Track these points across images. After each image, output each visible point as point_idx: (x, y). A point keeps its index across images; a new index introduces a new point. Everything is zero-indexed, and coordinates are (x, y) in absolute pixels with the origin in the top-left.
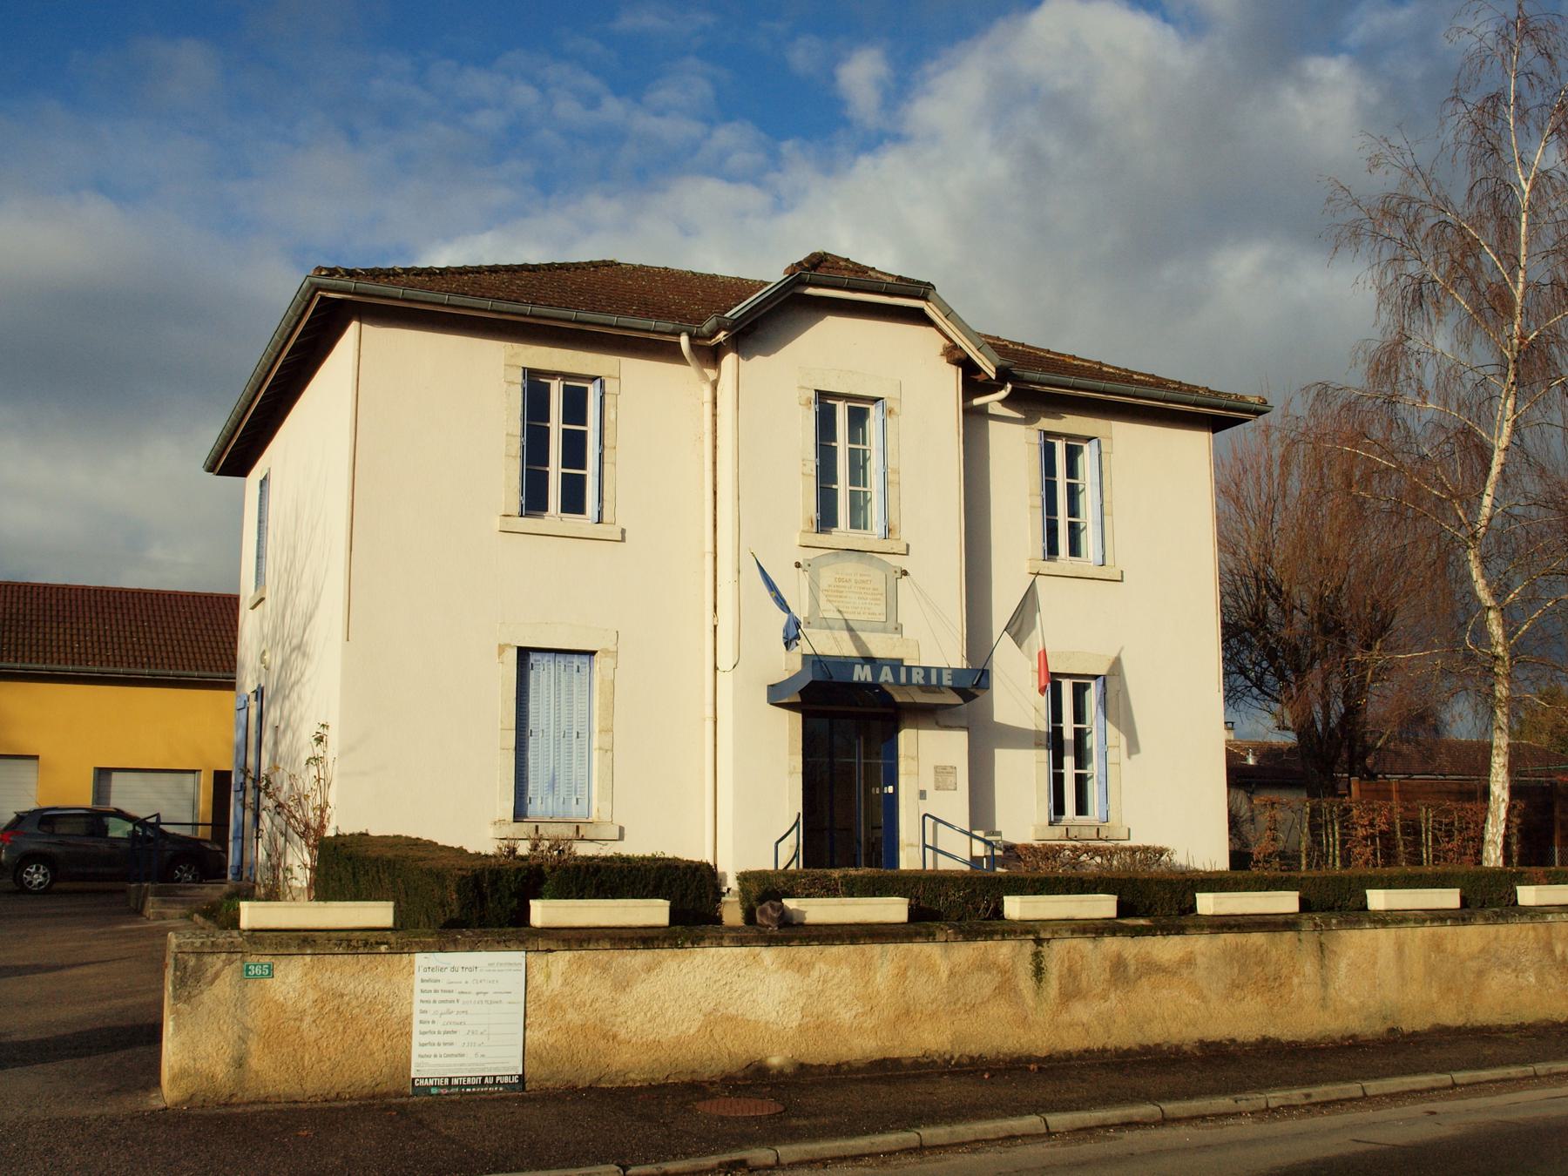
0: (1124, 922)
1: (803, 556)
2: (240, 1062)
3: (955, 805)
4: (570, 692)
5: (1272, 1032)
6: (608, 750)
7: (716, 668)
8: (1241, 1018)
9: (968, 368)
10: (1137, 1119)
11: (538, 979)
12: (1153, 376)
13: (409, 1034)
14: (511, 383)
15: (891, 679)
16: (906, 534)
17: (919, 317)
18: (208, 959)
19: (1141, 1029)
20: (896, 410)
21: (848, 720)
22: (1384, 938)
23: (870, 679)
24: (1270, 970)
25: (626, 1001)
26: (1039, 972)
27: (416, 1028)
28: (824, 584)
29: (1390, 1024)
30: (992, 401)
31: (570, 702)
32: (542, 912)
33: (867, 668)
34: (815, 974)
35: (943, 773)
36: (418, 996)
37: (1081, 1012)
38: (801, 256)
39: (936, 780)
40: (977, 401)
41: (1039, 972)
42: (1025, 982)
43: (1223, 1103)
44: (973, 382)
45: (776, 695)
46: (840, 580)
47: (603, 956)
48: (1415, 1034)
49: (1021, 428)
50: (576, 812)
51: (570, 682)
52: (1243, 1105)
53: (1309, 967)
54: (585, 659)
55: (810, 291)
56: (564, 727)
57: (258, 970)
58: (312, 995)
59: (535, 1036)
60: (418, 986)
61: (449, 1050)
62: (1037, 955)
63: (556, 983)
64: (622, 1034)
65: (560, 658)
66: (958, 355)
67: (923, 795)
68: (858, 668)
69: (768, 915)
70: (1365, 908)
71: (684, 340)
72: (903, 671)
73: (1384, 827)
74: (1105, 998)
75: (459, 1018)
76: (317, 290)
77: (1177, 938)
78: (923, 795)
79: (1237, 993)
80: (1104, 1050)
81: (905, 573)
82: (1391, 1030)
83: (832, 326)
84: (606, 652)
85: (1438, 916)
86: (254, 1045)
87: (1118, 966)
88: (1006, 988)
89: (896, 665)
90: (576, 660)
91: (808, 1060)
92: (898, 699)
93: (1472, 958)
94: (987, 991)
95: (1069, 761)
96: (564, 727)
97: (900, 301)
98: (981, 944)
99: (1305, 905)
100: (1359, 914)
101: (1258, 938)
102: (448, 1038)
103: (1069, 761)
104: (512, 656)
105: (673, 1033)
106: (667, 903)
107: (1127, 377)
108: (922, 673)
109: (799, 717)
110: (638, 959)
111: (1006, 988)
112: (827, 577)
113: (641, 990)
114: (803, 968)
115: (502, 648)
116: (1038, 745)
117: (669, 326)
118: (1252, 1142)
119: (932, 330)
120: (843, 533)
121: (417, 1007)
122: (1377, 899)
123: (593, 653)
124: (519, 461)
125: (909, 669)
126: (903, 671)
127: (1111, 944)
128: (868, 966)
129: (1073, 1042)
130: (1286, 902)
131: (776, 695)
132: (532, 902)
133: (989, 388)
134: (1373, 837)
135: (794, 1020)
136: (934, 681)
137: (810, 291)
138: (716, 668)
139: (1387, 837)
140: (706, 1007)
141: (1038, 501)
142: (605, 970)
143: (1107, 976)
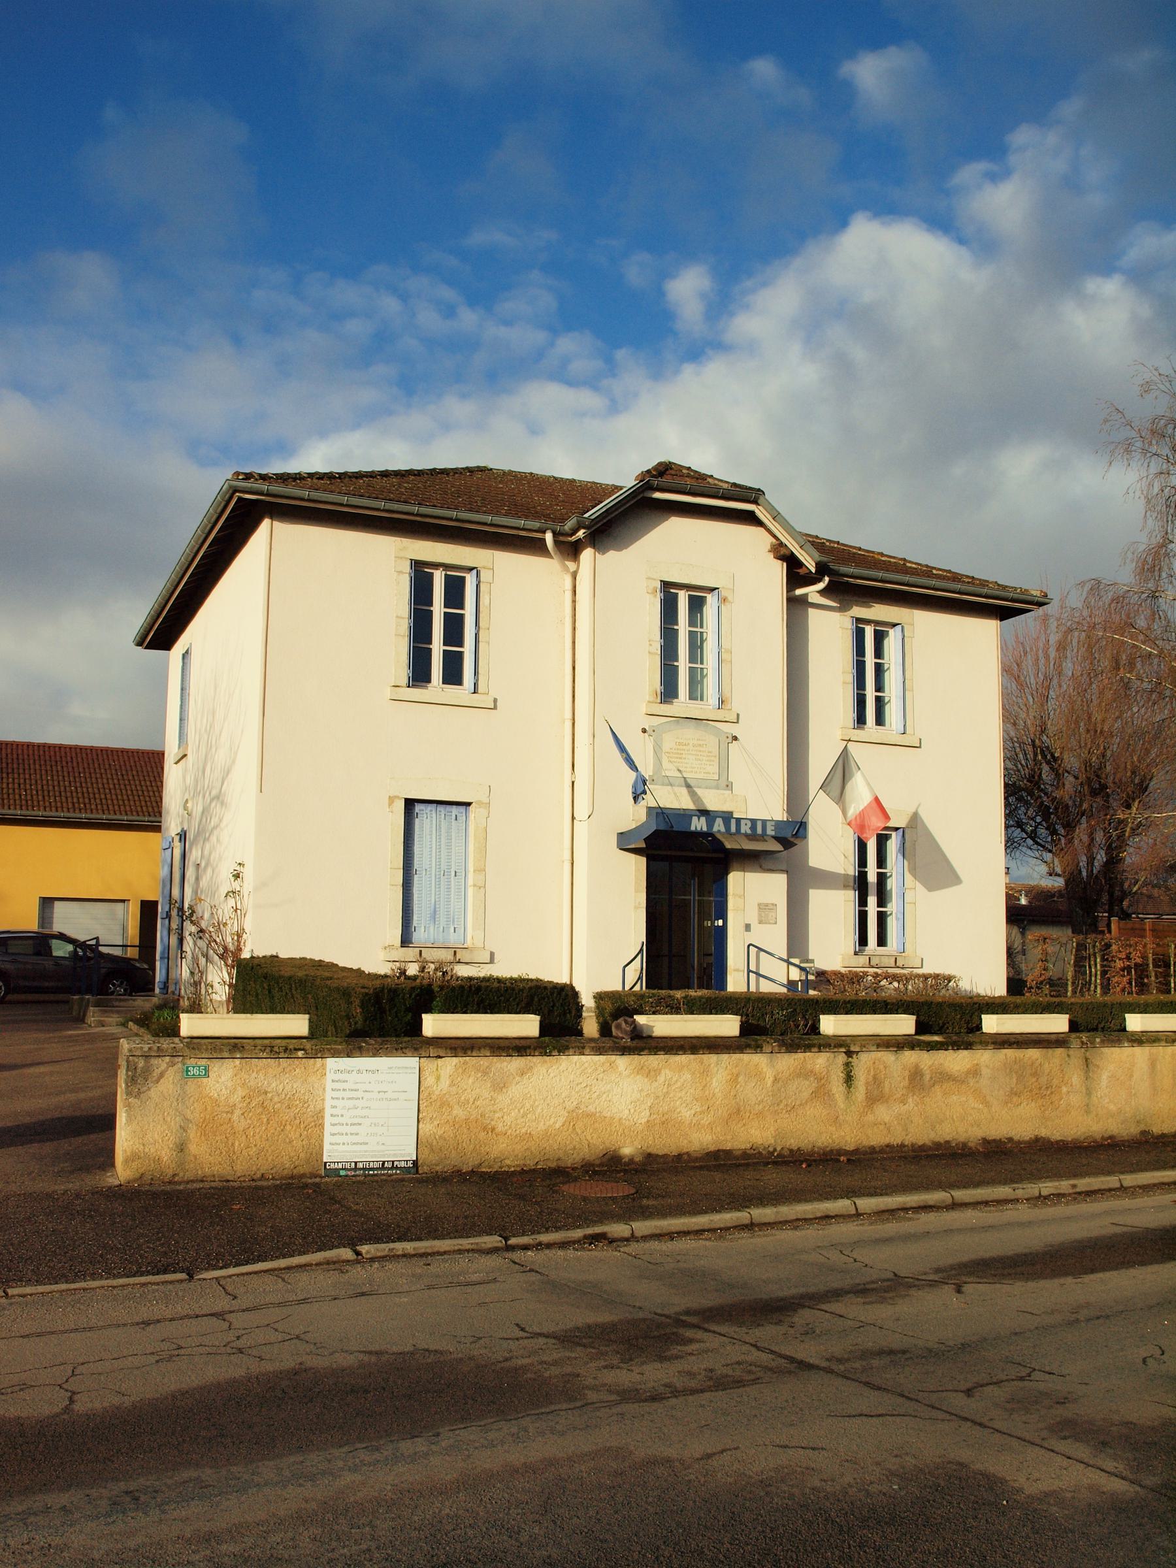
0: (922, 1038)
1: (649, 723)
2: (181, 1148)
3: (775, 937)
4: (449, 838)
5: (1044, 1133)
6: (481, 887)
7: (573, 818)
8: (1019, 1121)
9: (792, 562)
10: (931, 1203)
11: (429, 1080)
12: (949, 571)
13: (322, 1126)
14: (400, 572)
15: (723, 829)
16: (737, 705)
17: (750, 519)
18: (154, 1061)
19: (933, 1128)
20: (730, 598)
21: (686, 864)
22: (1140, 1054)
23: (705, 829)
24: (1043, 1080)
25: (503, 1099)
26: (849, 1079)
27: (328, 1120)
29: (1142, 1127)
30: (812, 592)
31: (449, 846)
32: (433, 1024)
33: (703, 819)
34: (661, 1079)
35: (765, 910)
36: (329, 1094)
37: (883, 1113)
38: (650, 465)
39: (760, 915)
40: (799, 592)
41: (849, 1079)
43: (1003, 1191)
44: (796, 575)
45: (625, 842)
46: (680, 744)
47: (484, 1062)
48: (1163, 1135)
49: (836, 616)
50: (453, 939)
51: (449, 828)
52: (1020, 1193)
53: (1076, 1079)
54: (462, 809)
55: (658, 495)
57: (196, 1071)
58: (240, 1092)
59: (427, 1128)
60: (329, 1085)
61: (355, 1139)
62: (847, 1064)
63: (445, 1084)
64: (500, 1128)
65: (441, 808)
66: (783, 551)
67: (748, 927)
68: (695, 819)
70: (1124, 1030)
71: (549, 537)
72: (733, 822)
73: (1139, 961)
74: (904, 1102)
75: (365, 1112)
76: (235, 491)
77: (965, 1052)
78: (748, 927)
79: (1015, 1099)
80: (902, 1145)
81: (735, 738)
82: (1143, 1133)
83: (676, 525)
84: (480, 803)
86: (193, 1133)
87: (915, 1077)
88: (821, 1092)
89: (727, 817)
90: (455, 810)
91: (654, 1150)
92: (728, 846)
94: (806, 1095)
95: (872, 901)
97: (735, 505)
98: (800, 1056)
99: (1074, 1026)
100: (1118, 1034)
101: (1033, 1054)
102: (355, 1129)
103: (872, 901)
104: (402, 804)
105: (541, 1127)
106: (538, 1018)
107: (928, 572)
109: (643, 860)
110: (514, 1064)
111: (821, 1092)
112: (668, 742)
113: (515, 1091)
114: (652, 1074)
115: (392, 800)
116: (845, 887)
117: (536, 525)
119: (761, 529)
120: (682, 704)
121: (328, 1103)
122: (1135, 1022)
123: (469, 804)
124: (407, 639)
125: (738, 820)
126: (733, 822)
127: (910, 1057)
128: (706, 1072)
129: (876, 1138)
130: (1058, 1023)
131: (625, 842)
132: (424, 1016)
133: (810, 580)
134: (1129, 968)
135: (643, 1117)
136: (759, 831)
137: (658, 495)
138: (573, 818)
139: (1141, 969)
140: (570, 1105)
141: (850, 677)
142: (485, 1073)
143: (906, 1083)
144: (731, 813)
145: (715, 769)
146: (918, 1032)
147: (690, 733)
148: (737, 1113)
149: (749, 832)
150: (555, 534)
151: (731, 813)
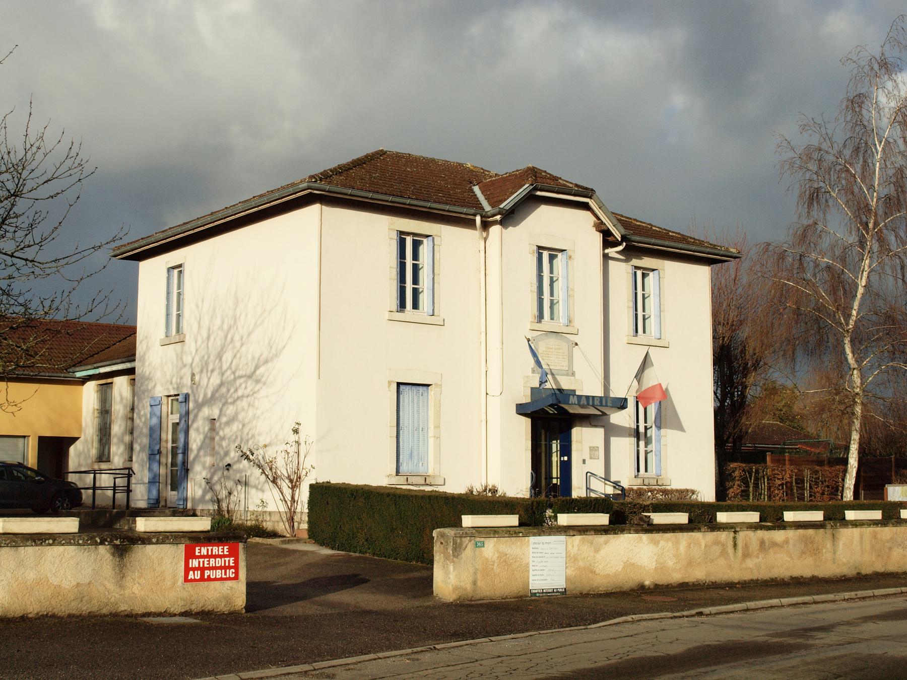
2: (474, 583)
3: (598, 468)
4: (418, 407)
5: (816, 573)
6: (437, 437)
8: (804, 568)
9: (606, 233)
11: (570, 547)
12: (679, 234)
13: (528, 571)
16: (577, 323)
17: (585, 207)
18: (464, 539)
21: (552, 420)
22: (856, 531)
24: (815, 545)
25: (599, 556)
26: (735, 545)
27: (531, 568)
30: (612, 252)
31: (418, 411)
34: (660, 545)
35: (593, 449)
36: (531, 555)
37: (750, 563)
40: (607, 251)
41: (735, 545)
42: (730, 549)
43: (830, 597)
44: (608, 241)
45: (521, 410)
47: (590, 537)
48: (866, 575)
49: (623, 264)
50: (421, 470)
51: (418, 400)
52: (837, 598)
53: (829, 545)
54: (425, 388)
55: (539, 193)
56: (416, 425)
58: (496, 555)
59: (569, 572)
60: (531, 550)
61: (542, 578)
62: (734, 538)
63: (576, 548)
64: (597, 572)
65: (414, 388)
66: (603, 228)
67: (584, 461)
69: (701, 517)
70: (844, 519)
71: (478, 219)
73: (789, 480)
74: (758, 557)
75: (546, 564)
77: (782, 531)
78: (584, 461)
80: (757, 580)
81: (576, 344)
82: (858, 574)
83: (544, 210)
84: (437, 385)
85: (875, 523)
86: (479, 576)
87: (762, 543)
88: (724, 553)
90: (421, 388)
91: (658, 583)
92: (571, 411)
93: (887, 542)
94: (718, 554)
95: (642, 443)
96: (416, 425)
97: (576, 197)
98: (715, 533)
99: (826, 518)
100: (845, 523)
101: (811, 532)
102: (542, 573)
103: (642, 443)
105: (614, 571)
107: (683, 239)
109: (529, 420)
110: (602, 538)
111: (724, 553)
113: (603, 552)
114: (656, 543)
115: (390, 383)
116: (630, 435)
117: (472, 211)
118: (860, 607)
119: (588, 213)
121: (531, 559)
122: (789, 516)
123: (428, 385)
124: (395, 282)
127: (760, 533)
128: (677, 542)
129: (747, 576)
130: (818, 516)
131: (521, 410)
133: (615, 244)
134: (782, 484)
135: (653, 565)
137: (539, 193)
139: (789, 486)
140: (625, 560)
141: (632, 304)
142: (591, 544)
143: (758, 547)
144: (574, 391)
145: (566, 363)
146: (761, 521)
147: (553, 341)
148: (690, 563)
150: (482, 217)
151: (574, 391)
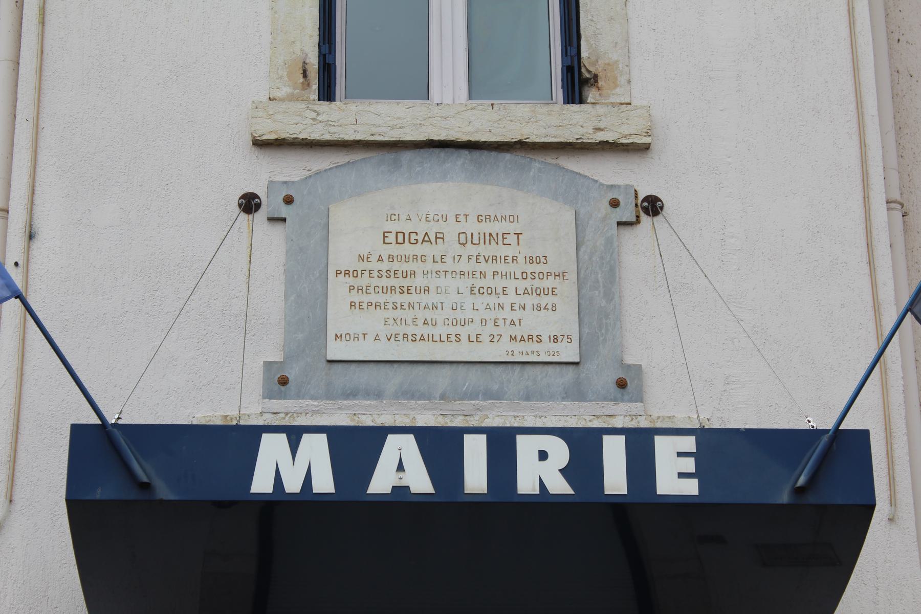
1: (263, 174)
15: (420, 482)
23: (324, 483)
28: (342, 253)
33: (316, 448)
46: (402, 238)
68: (272, 448)
81: (652, 206)
108: (560, 452)
136: (615, 479)
147: (446, 198)
149: (559, 486)
